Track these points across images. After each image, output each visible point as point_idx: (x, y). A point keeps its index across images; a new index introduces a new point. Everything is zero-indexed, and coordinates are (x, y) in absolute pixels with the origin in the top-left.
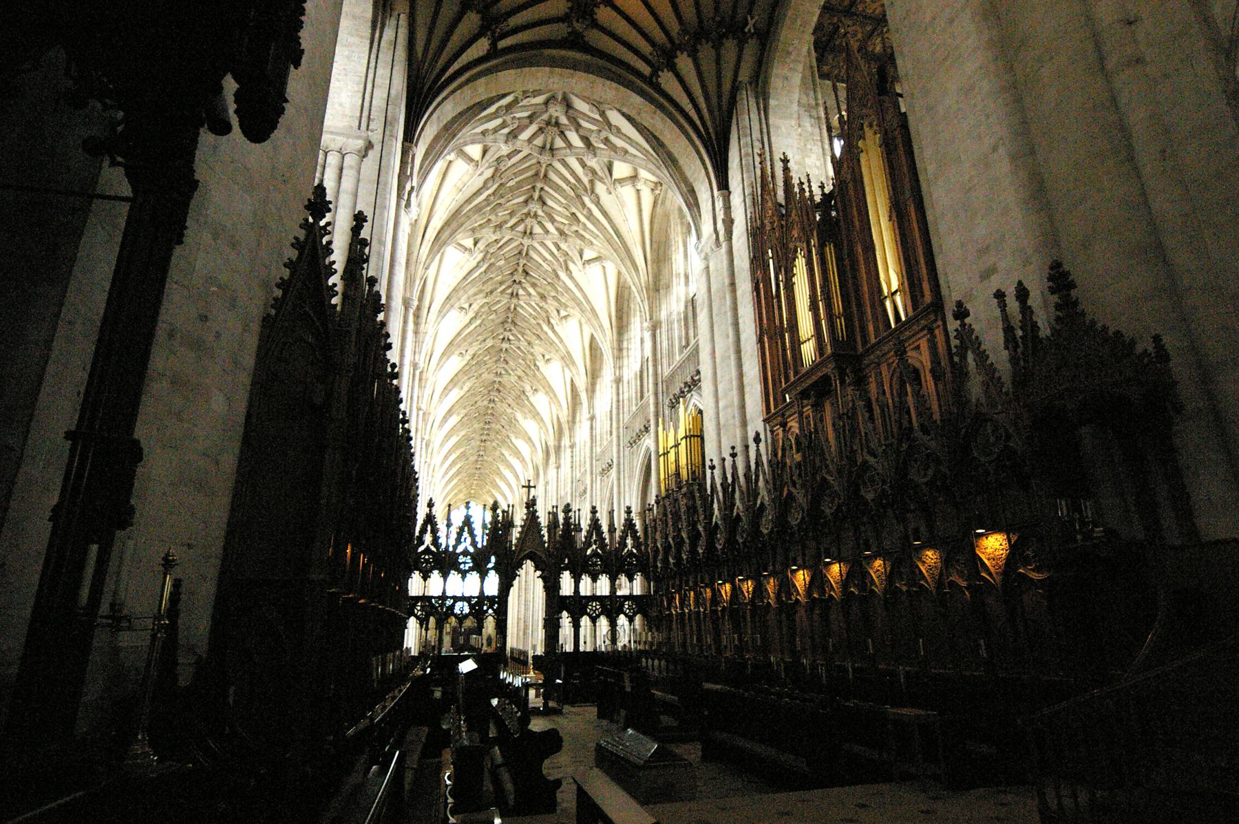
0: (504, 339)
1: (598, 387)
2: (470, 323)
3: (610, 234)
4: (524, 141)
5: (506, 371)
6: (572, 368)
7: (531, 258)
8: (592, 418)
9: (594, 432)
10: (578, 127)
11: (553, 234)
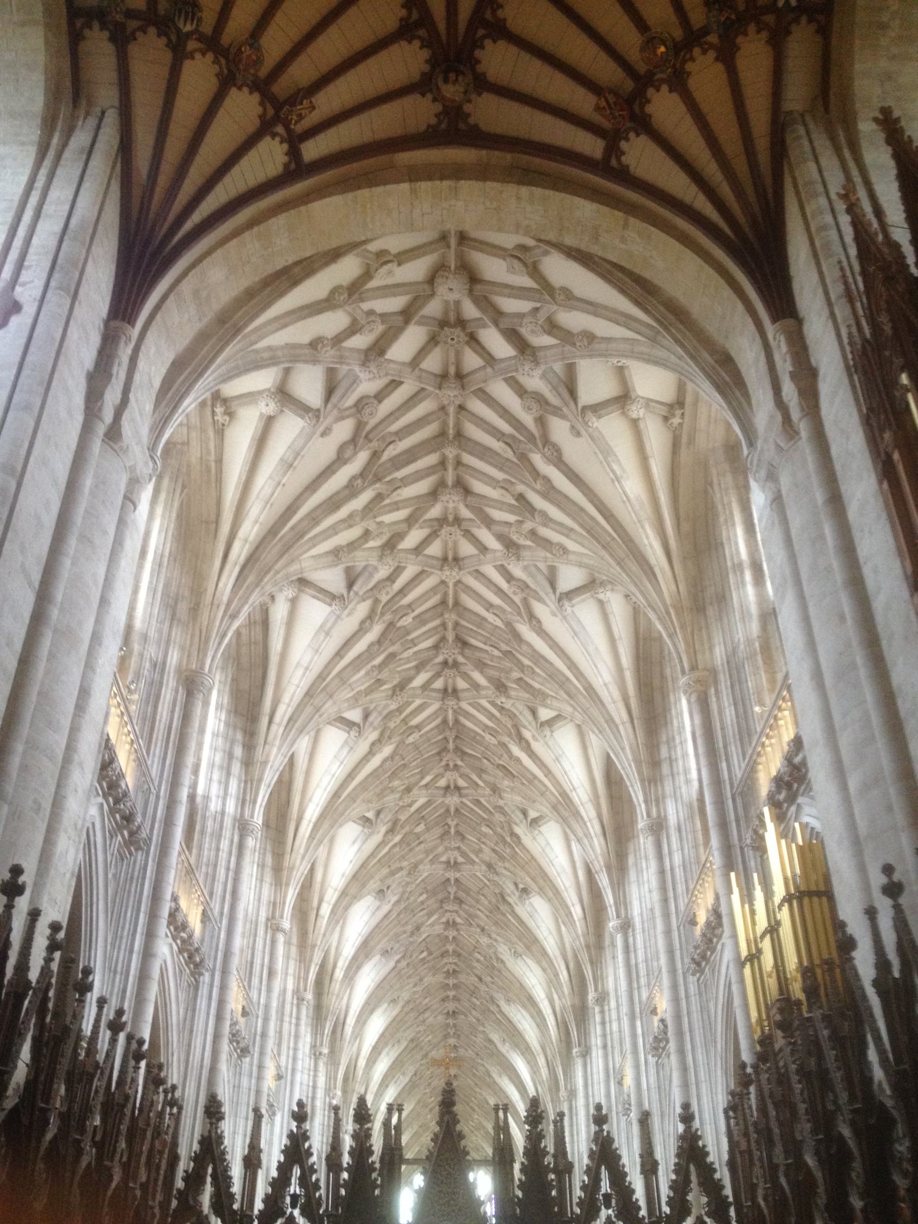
0: (447, 788)
1: (631, 860)
2: (371, 753)
3: (592, 518)
4: (404, 364)
5: (464, 854)
6: (575, 826)
7: (465, 609)
8: (626, 926)
9: (632, 956)
10: (497, 316)
11: (495, 551)
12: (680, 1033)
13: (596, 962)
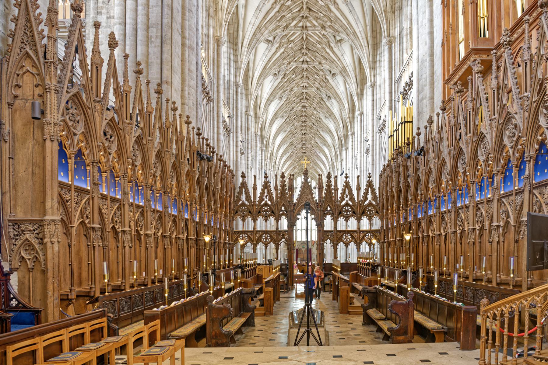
5: (309, 84)
8: (361, 114)
12: (373, 150)
13: (352, 123)
